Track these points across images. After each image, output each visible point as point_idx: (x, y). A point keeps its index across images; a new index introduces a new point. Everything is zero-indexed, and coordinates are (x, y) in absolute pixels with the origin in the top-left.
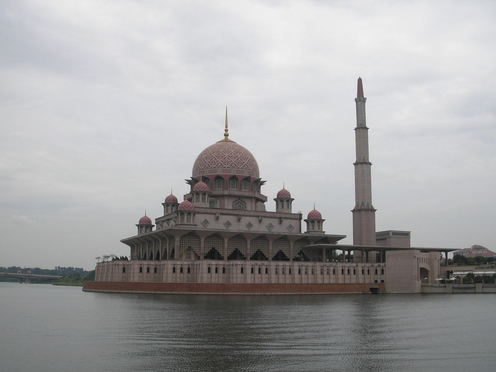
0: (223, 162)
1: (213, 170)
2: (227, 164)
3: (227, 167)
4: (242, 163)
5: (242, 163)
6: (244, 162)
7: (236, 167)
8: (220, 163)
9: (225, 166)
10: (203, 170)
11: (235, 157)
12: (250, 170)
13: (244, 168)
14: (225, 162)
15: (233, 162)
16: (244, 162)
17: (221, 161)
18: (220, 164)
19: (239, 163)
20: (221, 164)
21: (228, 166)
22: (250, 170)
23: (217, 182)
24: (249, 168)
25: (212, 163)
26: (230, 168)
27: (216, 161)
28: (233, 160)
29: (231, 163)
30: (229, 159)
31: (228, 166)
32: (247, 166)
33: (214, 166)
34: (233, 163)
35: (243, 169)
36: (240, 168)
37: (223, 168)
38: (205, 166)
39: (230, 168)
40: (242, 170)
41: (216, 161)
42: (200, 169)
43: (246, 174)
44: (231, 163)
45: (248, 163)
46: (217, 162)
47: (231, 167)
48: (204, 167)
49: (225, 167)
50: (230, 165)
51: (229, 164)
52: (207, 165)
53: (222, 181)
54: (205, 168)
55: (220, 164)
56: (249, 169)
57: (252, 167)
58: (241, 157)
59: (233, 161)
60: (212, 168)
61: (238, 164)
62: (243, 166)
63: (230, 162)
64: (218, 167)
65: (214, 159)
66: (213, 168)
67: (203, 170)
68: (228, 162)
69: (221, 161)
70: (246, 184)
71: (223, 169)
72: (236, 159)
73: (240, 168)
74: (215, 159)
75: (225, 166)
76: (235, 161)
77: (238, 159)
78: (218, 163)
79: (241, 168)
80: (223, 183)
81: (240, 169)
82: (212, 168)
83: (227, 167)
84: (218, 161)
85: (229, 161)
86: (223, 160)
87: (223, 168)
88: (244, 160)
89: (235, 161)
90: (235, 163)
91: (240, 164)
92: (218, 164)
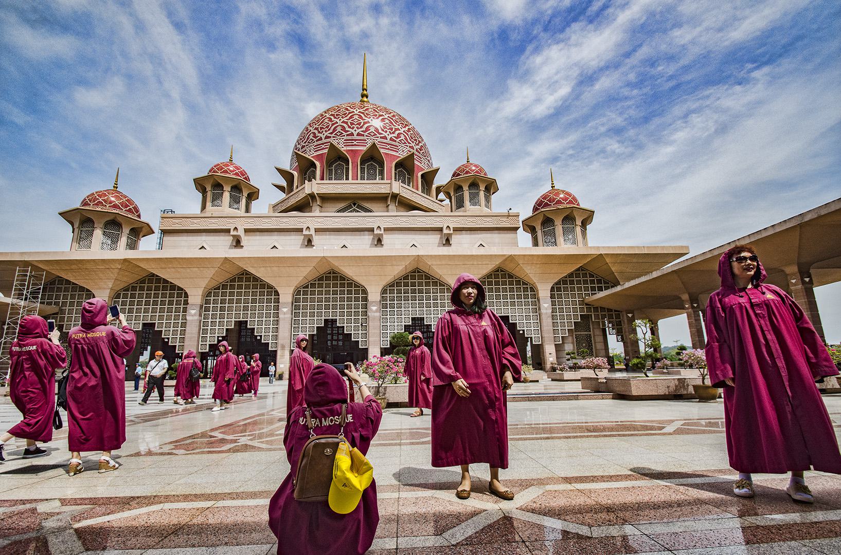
0: (346, 123)
3: (355, 133)
6: (398, 129)
14: (352, 124)
16: (398, 129)
18: (339, 129)
20: (343, 129)
25: (321, 128)
29: (366, 126)
36: (389, 138)
40: (394, 143)
43: (402, 154)
49: (352, 134)
50: (363, 129)
52: (311, 137)
55: (339, 129)
60: (321, 139)
63: (365, 123)
65: (326, 121)
68: (359, 124)
71: (345, 138)
73: (389, 138)
74: (330, 120)
75: (353, 131)
80: (348, 169)
81: (388, 141)
82: (321, 139)
83: (355, 133)
92: (334, 130)
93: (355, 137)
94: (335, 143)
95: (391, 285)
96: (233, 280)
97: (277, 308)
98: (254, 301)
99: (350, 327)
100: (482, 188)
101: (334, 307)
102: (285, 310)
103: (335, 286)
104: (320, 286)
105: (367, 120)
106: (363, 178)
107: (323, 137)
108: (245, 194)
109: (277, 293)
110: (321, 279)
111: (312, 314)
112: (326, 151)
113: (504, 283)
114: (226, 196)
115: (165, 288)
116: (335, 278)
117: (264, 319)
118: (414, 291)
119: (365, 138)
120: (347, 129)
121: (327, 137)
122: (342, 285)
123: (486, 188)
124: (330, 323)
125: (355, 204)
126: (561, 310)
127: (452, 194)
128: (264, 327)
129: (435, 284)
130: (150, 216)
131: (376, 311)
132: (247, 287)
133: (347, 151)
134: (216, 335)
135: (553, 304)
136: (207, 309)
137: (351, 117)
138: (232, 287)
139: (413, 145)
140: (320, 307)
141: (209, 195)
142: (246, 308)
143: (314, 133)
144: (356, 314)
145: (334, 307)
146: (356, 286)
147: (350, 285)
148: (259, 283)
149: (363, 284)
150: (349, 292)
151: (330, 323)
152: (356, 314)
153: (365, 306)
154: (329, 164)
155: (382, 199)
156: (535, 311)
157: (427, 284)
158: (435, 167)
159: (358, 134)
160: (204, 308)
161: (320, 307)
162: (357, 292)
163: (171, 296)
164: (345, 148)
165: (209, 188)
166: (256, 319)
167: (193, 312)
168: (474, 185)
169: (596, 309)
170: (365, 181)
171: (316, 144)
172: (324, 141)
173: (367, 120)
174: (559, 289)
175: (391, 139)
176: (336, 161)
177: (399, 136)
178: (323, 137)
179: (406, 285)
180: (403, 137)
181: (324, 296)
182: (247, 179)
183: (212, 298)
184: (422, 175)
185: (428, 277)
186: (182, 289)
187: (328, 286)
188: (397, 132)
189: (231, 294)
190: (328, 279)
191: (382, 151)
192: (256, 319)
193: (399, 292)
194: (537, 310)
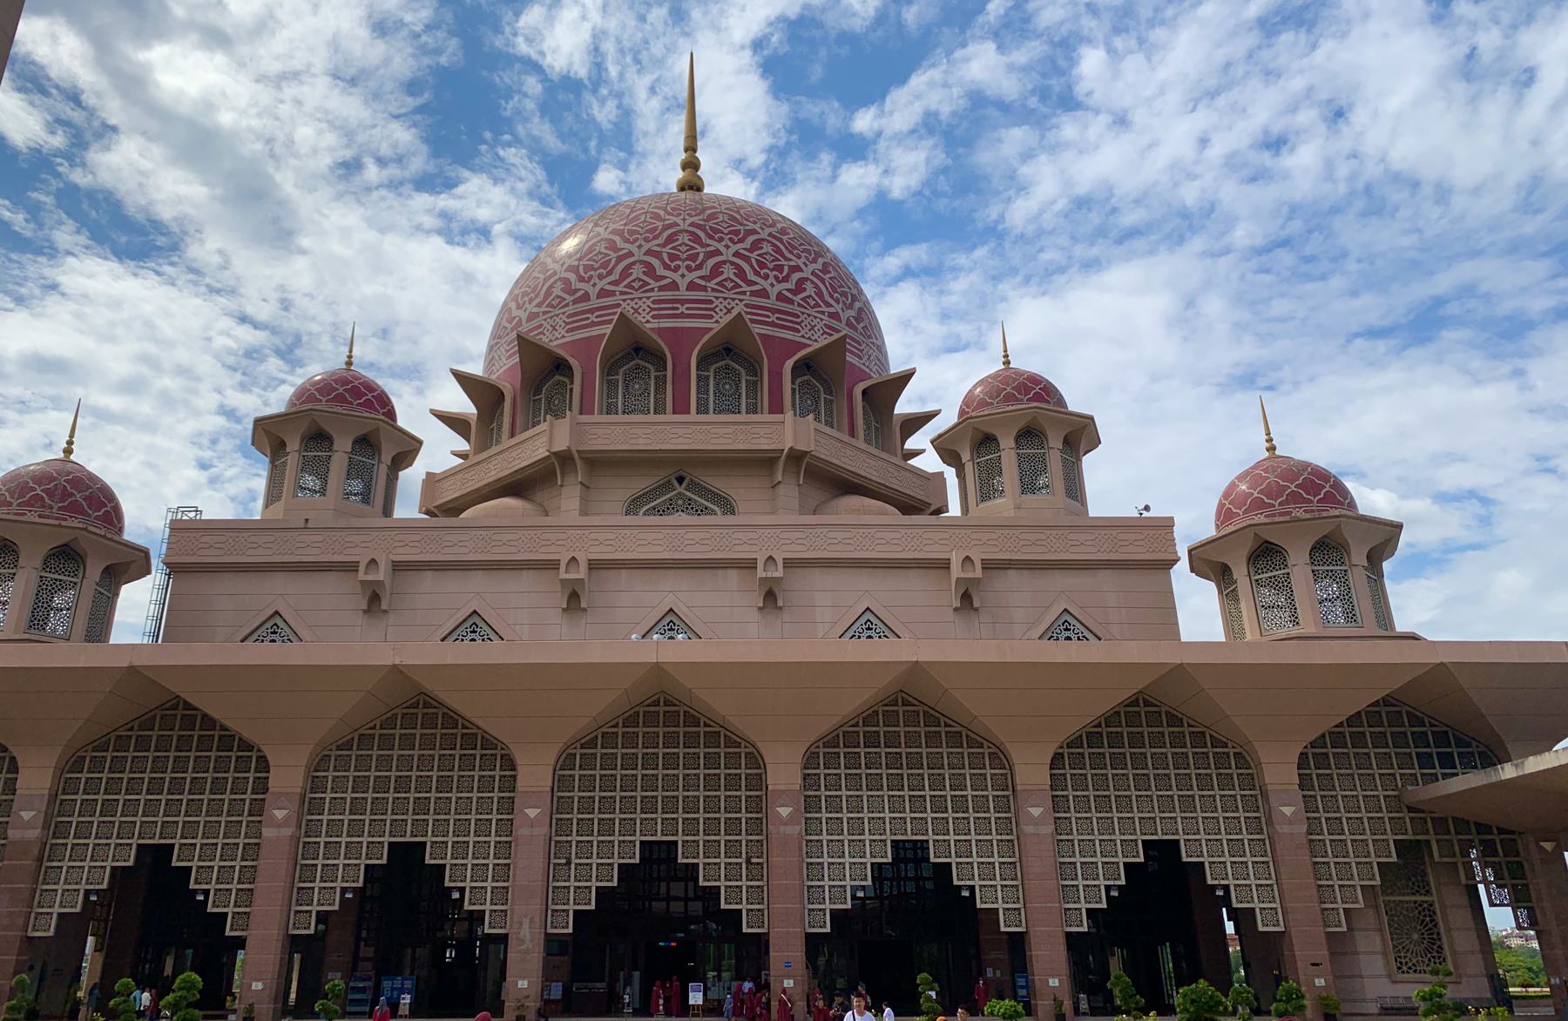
0: (657, 255)
1: (591, 311)
2: (689, 268)
4: (786, 269)
5: (786, 269)
6: (797, 269)
7: (745, 288)
8: (642, 262)
9: (676, 277)
10: (535, 323)
11: (737, 233)
12: (835, 316)
13: (797, 299)
15: (728, 255)
16: (797, 269)
17: (649, 252)
19: (762, 265)
20: (650, 270)
21: (690, 276)
22: (835, 316)
23: (620, 377)
24: (830, 306)
26: (704, 289)
27: (613, 255)
28: (727, 247)
30: (697, 239)
31: (690, 276)
32: (819, 294)
33: (601, 284)
34: (724, 262)
35: (791, 302)
36: (773, 293)
37: (661, 289)
38: (548, 293)
39: (704, 289)
41: (613, 255)
42: (520, 323)
44: (711, 262)
45: (823, 281)
46: (620, 259)
47: (712, 284)
48: (539, 305)
49: (674, 286)
50: (705, 272)
51: (699, 267)
53: (653, 374)
54: (544, 309)
55: (637, 271)
56: (832, 310)
57: (850, 307)
58: (781, 240)
59: (723, 249)
61: (757, 273)
62: (791, 285)
64: (629, 286)
66: (593, 296)
67: (535, 323)
68: (693, 258)
69: (649, 252)
70: (817, 402)
71: (656, 295)
72: (747, 244)
73: (773, 293)
75: (676, 277)
76: (736, 254)
77: (756, 246)
78: (629, 266)
79: (780, 297)
80: (661, 381)
81: (771, 302)
84: (631, 254)
85: (699, 249)
86: (664, 245)
87: (661, 289)
88: (799, 257)
89: (736, 254)
90: (737, 266)
91: (772, 274)
92: (625, 273)
93: (683, 293)
94: (630, 313)
95: (830, 741)
96: (389, 723)
97: (508, 806)
98: (444, 784)
99: (717, 870)
100: (1055, 442)
101: (670, 805)
102: (532, 813)
103: (671, 740)
104: (630, 740)
105: (714, 245)
106: (702, 408)
107: (593, 293)
108: (387, 458)
109: (509, 763)
110: (631, 721)
111: (607, 827)
112: (607, 330)
113: (1158, 741)
114: (339, 462)
115: (204, 744)
116: (672, 718)
117: (472, 839)
118: (894, 760)
119: (710, 295)
120: (660, 271)
121: (603, 293)
122: (691, 740)
123: (1066, 441)
124: (659, 855)
125: (680, 480)
126: (1335, 825)
127: (966, 456)
128: (470, 861)
129: (955, 739)
130: (144, 521)
131: (791, 820)
132: (428, 743)
133: (659, 331)
134: (339, 884)
135: (1309, 804)
136: (316, 807)
137: (670, 239)
138: (386, 742)
139: (838, 308)
140: (628, 805)
141: (292, 460)
142: (421, 806)
143: (567, 282)
144: (733, 826)
145: (670, 805)
146: (730, 743)
147: (713, 739)
148: (459, 731)
149: (753, 738)
150: (712, 761)
151: (659, 855)
152: (733, 826)
153: (757, 805)
154: (610, 368)
155: (761, 463)
156: (1255, 826)
157: (933, 739)
158: (896, 367)
159: (692, 286)
160: (309, 804)
161: (628, 805)
162: (733, 761)
163: (221, 766)
164: (654, 324)
165: (293, 445)
166: (450, 839)
167: (280, 814)
168: (1029, 434)
169: (1441, 824)
170: (711, 417)
171: (571, 309)
172: (595, 302)
173: (714, 245)
174: (1322, 760)
175: (780, 297)
176: (627, 357)
177: (799, 288)
178: (593, 293)
179: (872, 740)
180: (810, 290)
181: (639, 772)
182: (391, 414)
183: (331, 774)
184: (864, 392)
185: (932, 718)
186: (250, 748)
187: (651, 741)
188: (796, 276)
189: (385, 763)
190: (651, 720)
191: (757, 329)
192: (450, 839)
193: (853, 760)
194: (1263, 822)
